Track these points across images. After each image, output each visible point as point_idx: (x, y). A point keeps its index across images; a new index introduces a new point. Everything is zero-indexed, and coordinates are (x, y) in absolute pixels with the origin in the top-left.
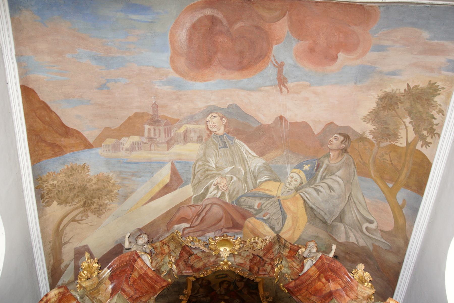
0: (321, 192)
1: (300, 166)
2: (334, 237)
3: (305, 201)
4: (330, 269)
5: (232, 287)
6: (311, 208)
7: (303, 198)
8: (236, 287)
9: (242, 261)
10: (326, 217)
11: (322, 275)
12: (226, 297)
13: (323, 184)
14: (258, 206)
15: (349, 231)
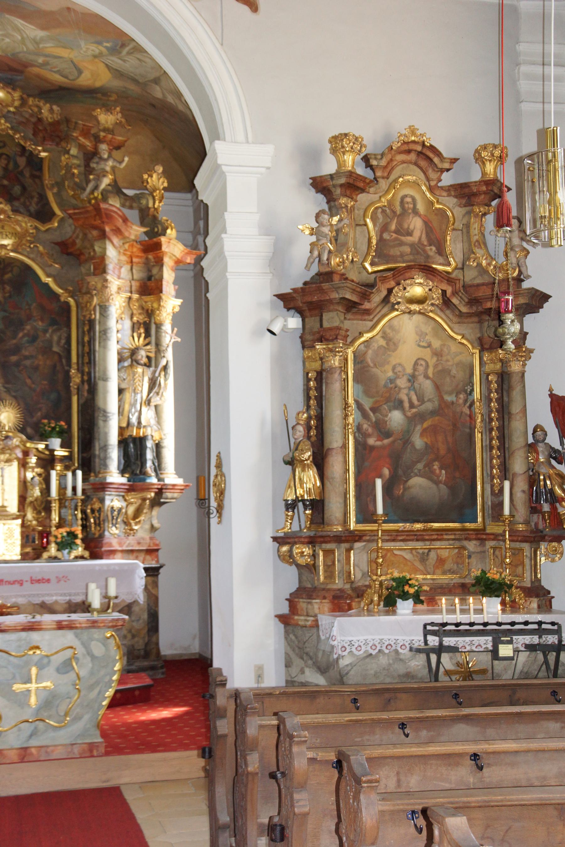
0: (128, 61)
1: (99, 43)
2: (149, 91)
3: (107, 66)
4: (106, 214)
5: (11, 166)
6: (116, 70)
7: (104, 63)
8: (16, 165)
9: (24, 120)
10: (137, 78)
11: (97, 217)
12: (5, 182)
13: (131, 57)
14: (43, 61)
15: (167, 94)
